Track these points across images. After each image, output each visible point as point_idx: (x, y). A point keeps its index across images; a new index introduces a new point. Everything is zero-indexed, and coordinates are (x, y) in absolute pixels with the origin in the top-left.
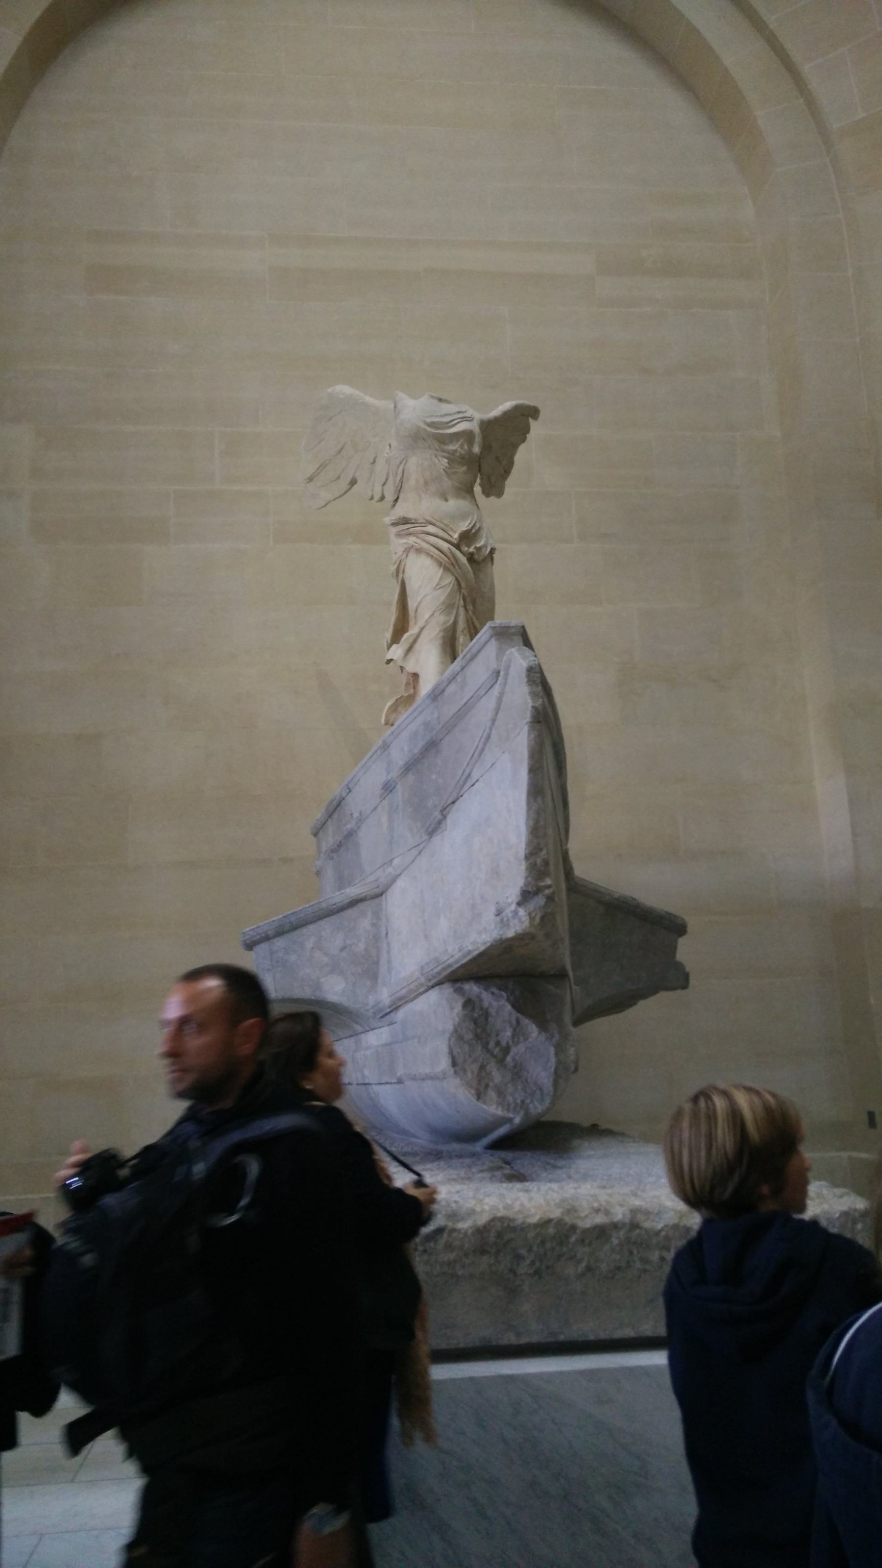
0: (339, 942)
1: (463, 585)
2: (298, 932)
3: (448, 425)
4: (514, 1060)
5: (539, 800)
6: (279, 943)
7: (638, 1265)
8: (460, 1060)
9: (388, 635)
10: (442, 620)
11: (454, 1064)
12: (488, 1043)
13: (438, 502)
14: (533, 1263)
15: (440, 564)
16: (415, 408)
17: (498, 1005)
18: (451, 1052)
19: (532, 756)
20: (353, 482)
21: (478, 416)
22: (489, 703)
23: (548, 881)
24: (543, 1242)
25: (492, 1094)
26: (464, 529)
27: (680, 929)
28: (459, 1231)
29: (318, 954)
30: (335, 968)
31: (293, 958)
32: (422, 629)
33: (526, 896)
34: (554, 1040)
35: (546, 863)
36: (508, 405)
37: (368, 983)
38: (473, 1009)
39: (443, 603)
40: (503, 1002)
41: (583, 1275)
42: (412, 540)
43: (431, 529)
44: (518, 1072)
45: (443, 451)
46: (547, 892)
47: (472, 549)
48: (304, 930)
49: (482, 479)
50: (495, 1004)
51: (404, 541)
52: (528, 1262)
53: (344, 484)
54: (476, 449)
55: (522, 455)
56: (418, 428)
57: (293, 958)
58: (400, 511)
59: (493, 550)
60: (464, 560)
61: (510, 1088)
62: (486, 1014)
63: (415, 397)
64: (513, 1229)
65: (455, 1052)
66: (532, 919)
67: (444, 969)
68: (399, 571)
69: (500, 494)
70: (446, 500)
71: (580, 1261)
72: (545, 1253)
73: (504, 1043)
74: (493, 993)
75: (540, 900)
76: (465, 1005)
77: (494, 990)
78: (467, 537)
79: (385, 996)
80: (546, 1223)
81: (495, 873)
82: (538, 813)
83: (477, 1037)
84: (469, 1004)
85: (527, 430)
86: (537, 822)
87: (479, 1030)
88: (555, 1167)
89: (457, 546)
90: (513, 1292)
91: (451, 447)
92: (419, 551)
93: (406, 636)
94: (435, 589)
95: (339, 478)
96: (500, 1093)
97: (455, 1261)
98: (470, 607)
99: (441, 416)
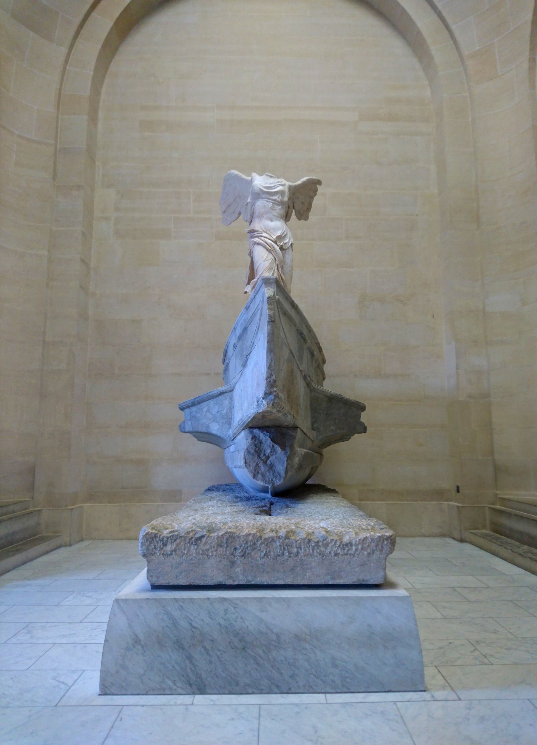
1: (277, 259)
2: (201, 404)
4: (270, 462)
5: (272, 355)
6: (194, 409)
7: (287, 554)
8: (248, 461)
9: (247, 281)
11: (246, 463)
12: (260, 454)
14: (242, 551)
15: (267, 250)
18: (245, 458)
19: (269, 335)
20: (240, 214)
21: (287, 183)
23: (275, 389)
24: (247, 543)
25: (260, 476)
26: (279, 235)
27: (363, 408)
28: (211, 537)
29: (208, 414)
30: (214, 420)
31: (198, 415)
33: (266, 395)
34: (287, 455)
35: (275, 381)
36: (305, 179)
37: (228, 426)
38: (255, 441)
39: (267, 267)
40: (268, 438)
41: (263, 558)
44: (271, 467)
46: (274, 393)
48: (203, 404)
49: (295, 212)
50: (264, 438)
52: (240, 551)
53: (236, 214)
54: (286, 199)
55: (317, 202)
56: (260, 189)
57: (198, 415)
60: (277, 248)
61: (268, 474)
62: (261, 443)
64: (234, 538)
65: (246, 458)
66: (268, 404)
67: (244, 423)
68: (251, 254)
69: (306, 219)
70: (272, 221)
71: (262, 552)
72: (247, 548)
73: (267, 455)
74: (264, 434)
75: (272, 397)
76: (252, 439)
77: (265, 433)
79: (231, 432)
80: (248, 535)
81: (258, 384)
82: (272, 360)
83: (256, 451)
84: (254, 438)
86: (271, 364)
87: (257, 449)
88: (287, 507)
89: (275, 242)
90: (233, 563)
91: (274, 198)
92: (259, 244)
94: (264, 261)
96: (263, 476)
97: (209, 549)
98: (280, 269)
99: (271, 184)
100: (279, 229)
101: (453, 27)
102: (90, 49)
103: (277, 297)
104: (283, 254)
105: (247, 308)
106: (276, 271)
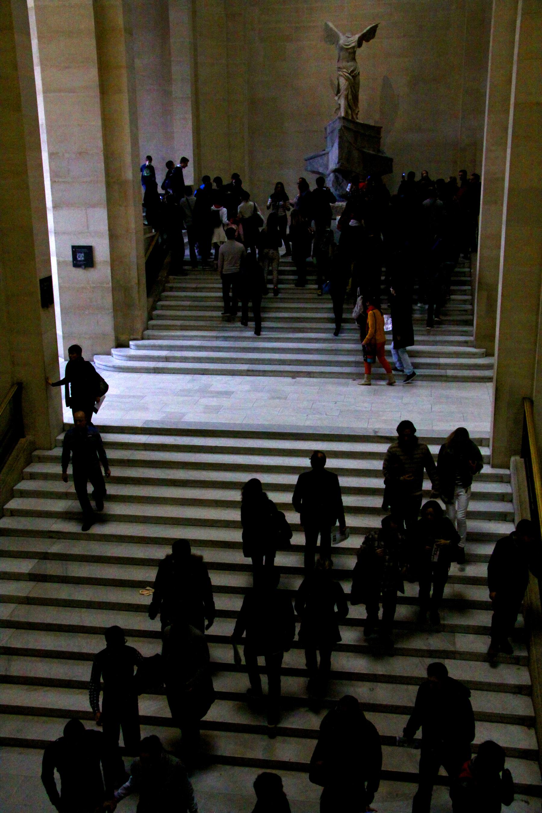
0: (321, 161)
6: (311, 161)
17: (340, 177)
33: (338, 163)
36: (368, 28)
42: (341, 73)
59: (359, 73)
60: (351, 77)
68: (338, 79)
78: (352, 72)
79: (328, 172)
89: (350, 74)
91: (350, 51)
92: (342, 76)
96: (339, 190)
98: (352, 88)
100: (351, 66)
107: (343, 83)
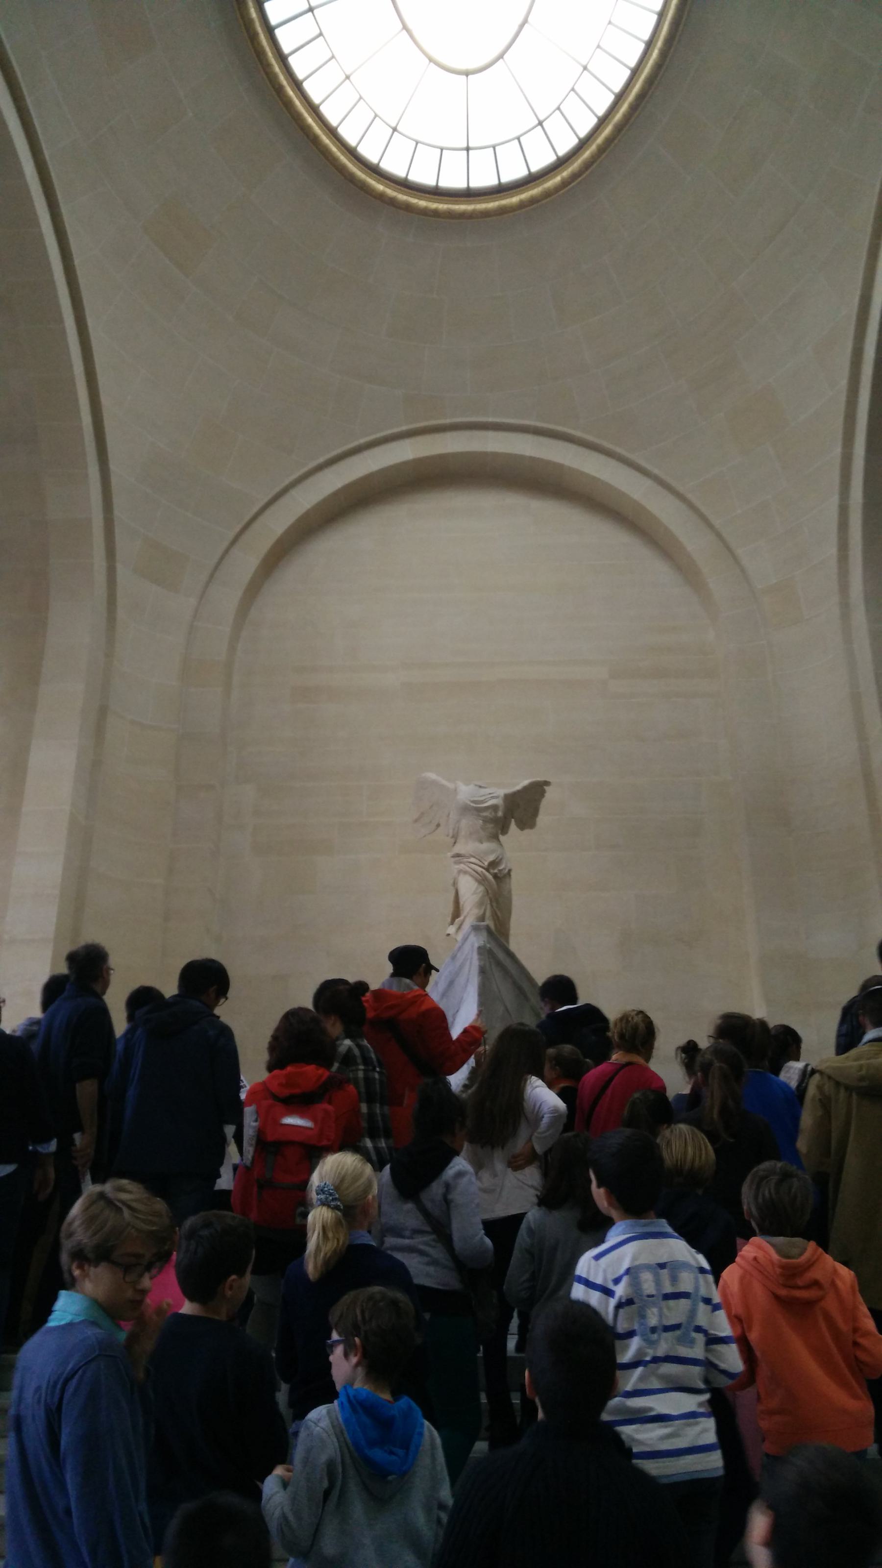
3: (482, 802)
9: (449, 919)
10: (476, 912)
13: (477, 844)
15: (476, 880)
16: (465, 792)
19: (479, 988)
20: (438, 825)
22: (468, 963)
32: (465, 917)
36: (526, 782)
42: (462, 866)
43: (473, 860)
45: (479, 816)
47: (496, 871)
51: (457, 867)
54: (500, 814)
58: (458, 849)
59: (510, 871)
60: (490, 877)
63: (467, 785)
68: (455, 884)
78: (493, 864)
85: (544, 792)
89: (487, 870)
91: (485, 814)
92: (465, 872)
93: (457, 920)
95: (431, 822)
98: (494, 904)
101: (739, 552)
102: (227, 598)
103: (488, 945)
104: (497, 884)
105: (454, 958)
106: (489, 907)
107: (470, 891)
